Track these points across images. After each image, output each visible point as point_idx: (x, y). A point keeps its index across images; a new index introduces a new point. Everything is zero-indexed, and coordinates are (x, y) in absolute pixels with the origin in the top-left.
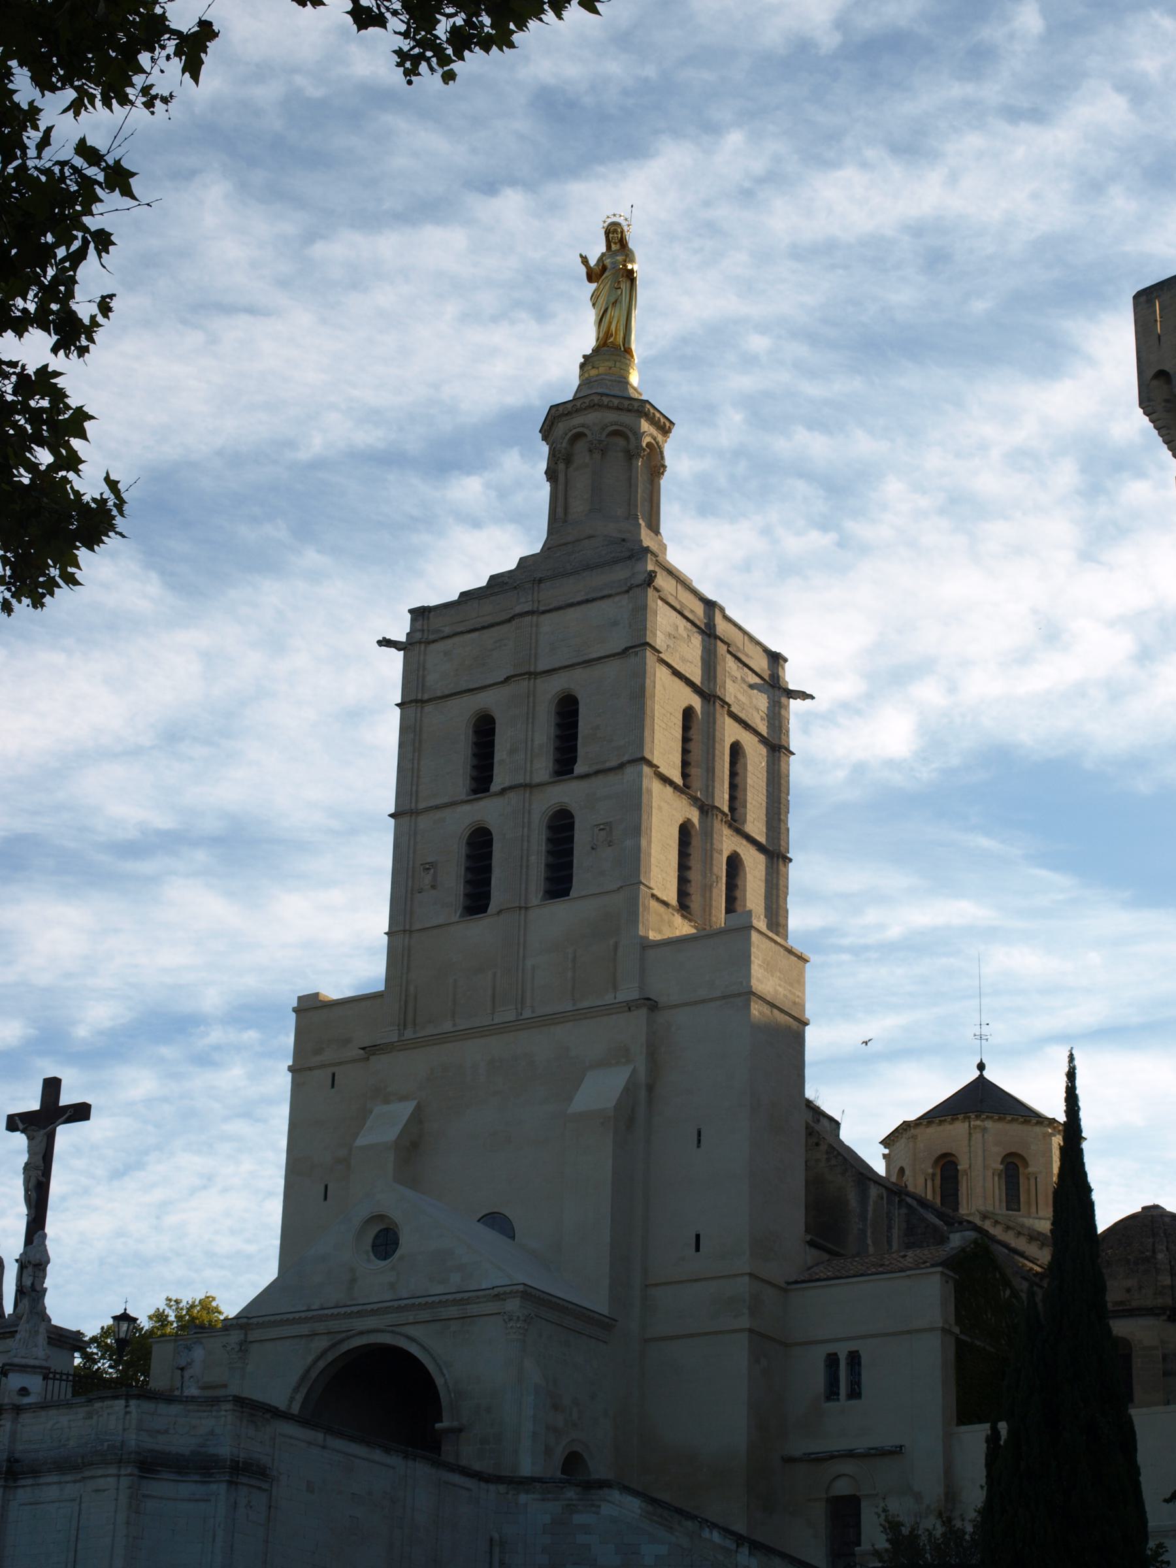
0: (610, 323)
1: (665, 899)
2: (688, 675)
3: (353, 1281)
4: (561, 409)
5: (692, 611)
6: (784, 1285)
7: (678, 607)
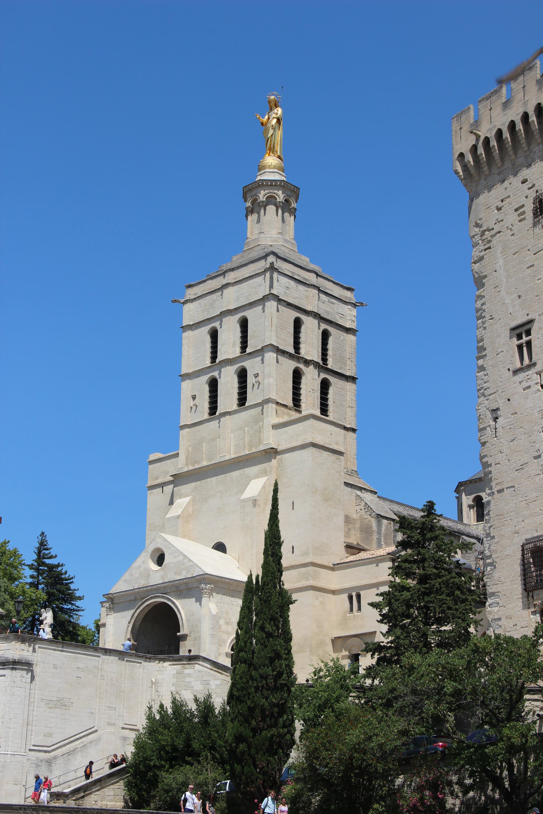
0: (271, 145)
1: (285, 404)
2: (296, 304)
3: (149, 575)
4: (250, 186)
5: (298, 275)
6: (332, 566)
7: (290, 275)
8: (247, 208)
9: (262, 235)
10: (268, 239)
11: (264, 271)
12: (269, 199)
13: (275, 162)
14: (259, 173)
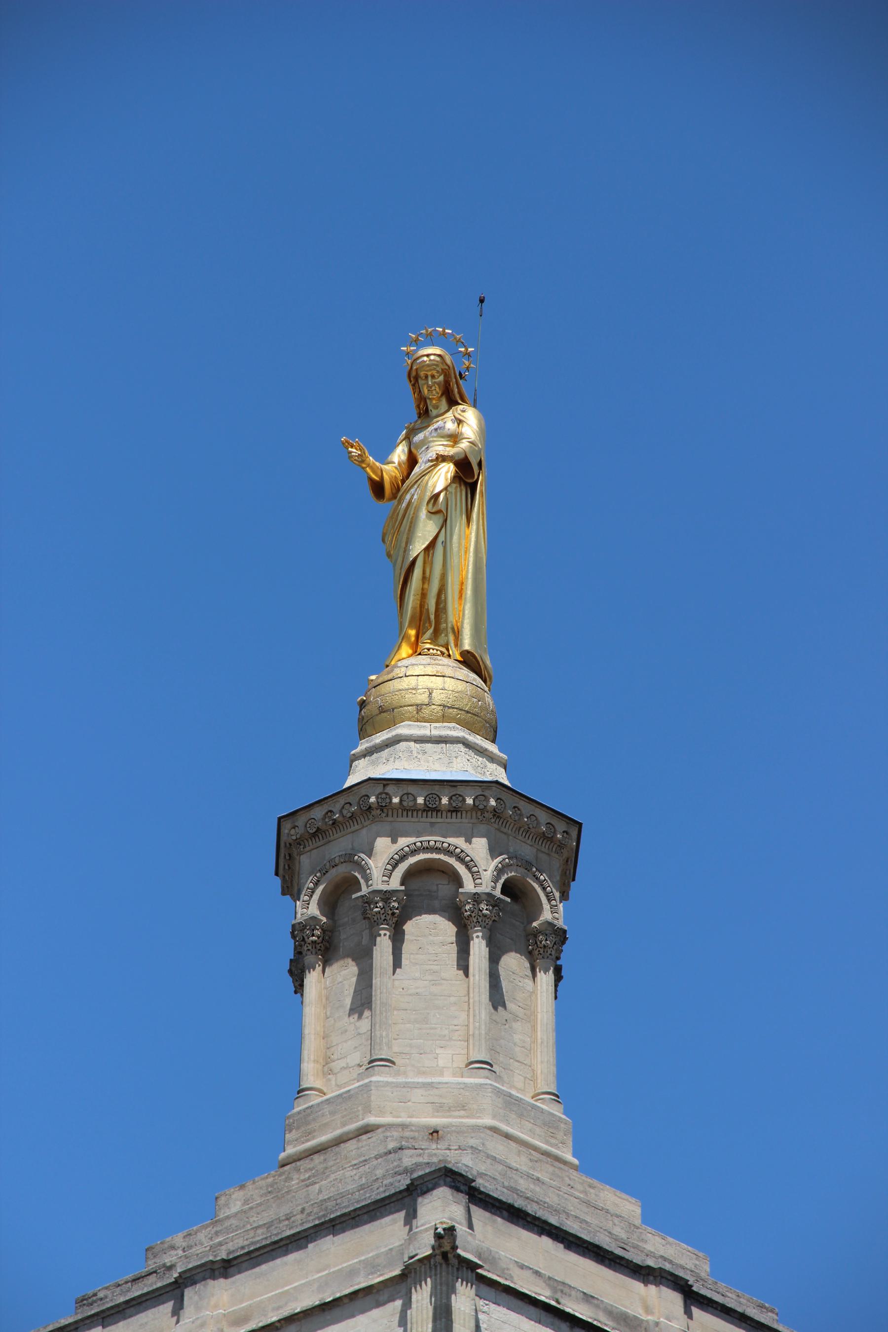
5: (588, 1298)
7: (544, 1295)
8: (298, 931)
9: (380, 1077)
10: (418, 1095)
11: (404, 1276)
12: (416, 884)
13: (450, 684)
14: (363, 745)
